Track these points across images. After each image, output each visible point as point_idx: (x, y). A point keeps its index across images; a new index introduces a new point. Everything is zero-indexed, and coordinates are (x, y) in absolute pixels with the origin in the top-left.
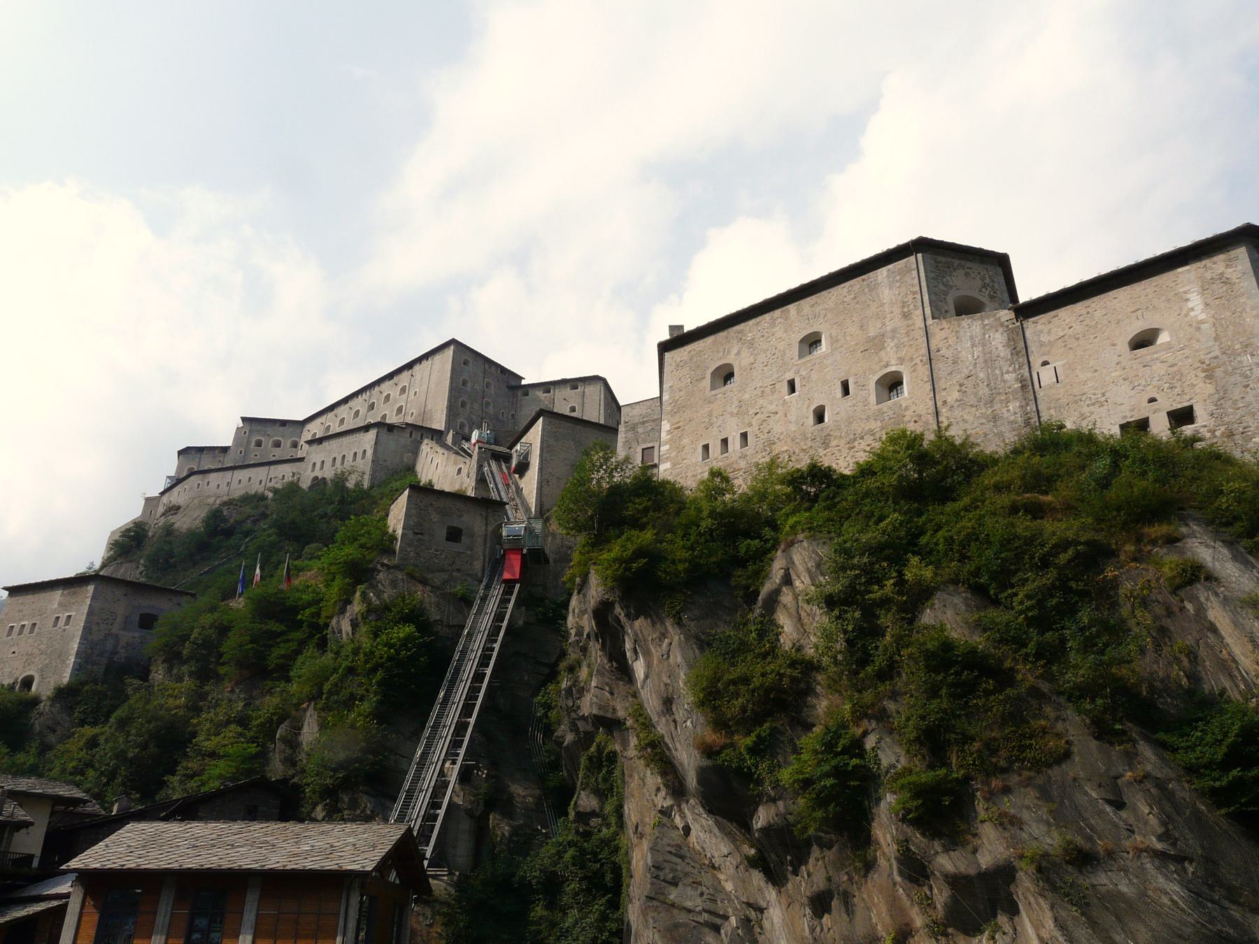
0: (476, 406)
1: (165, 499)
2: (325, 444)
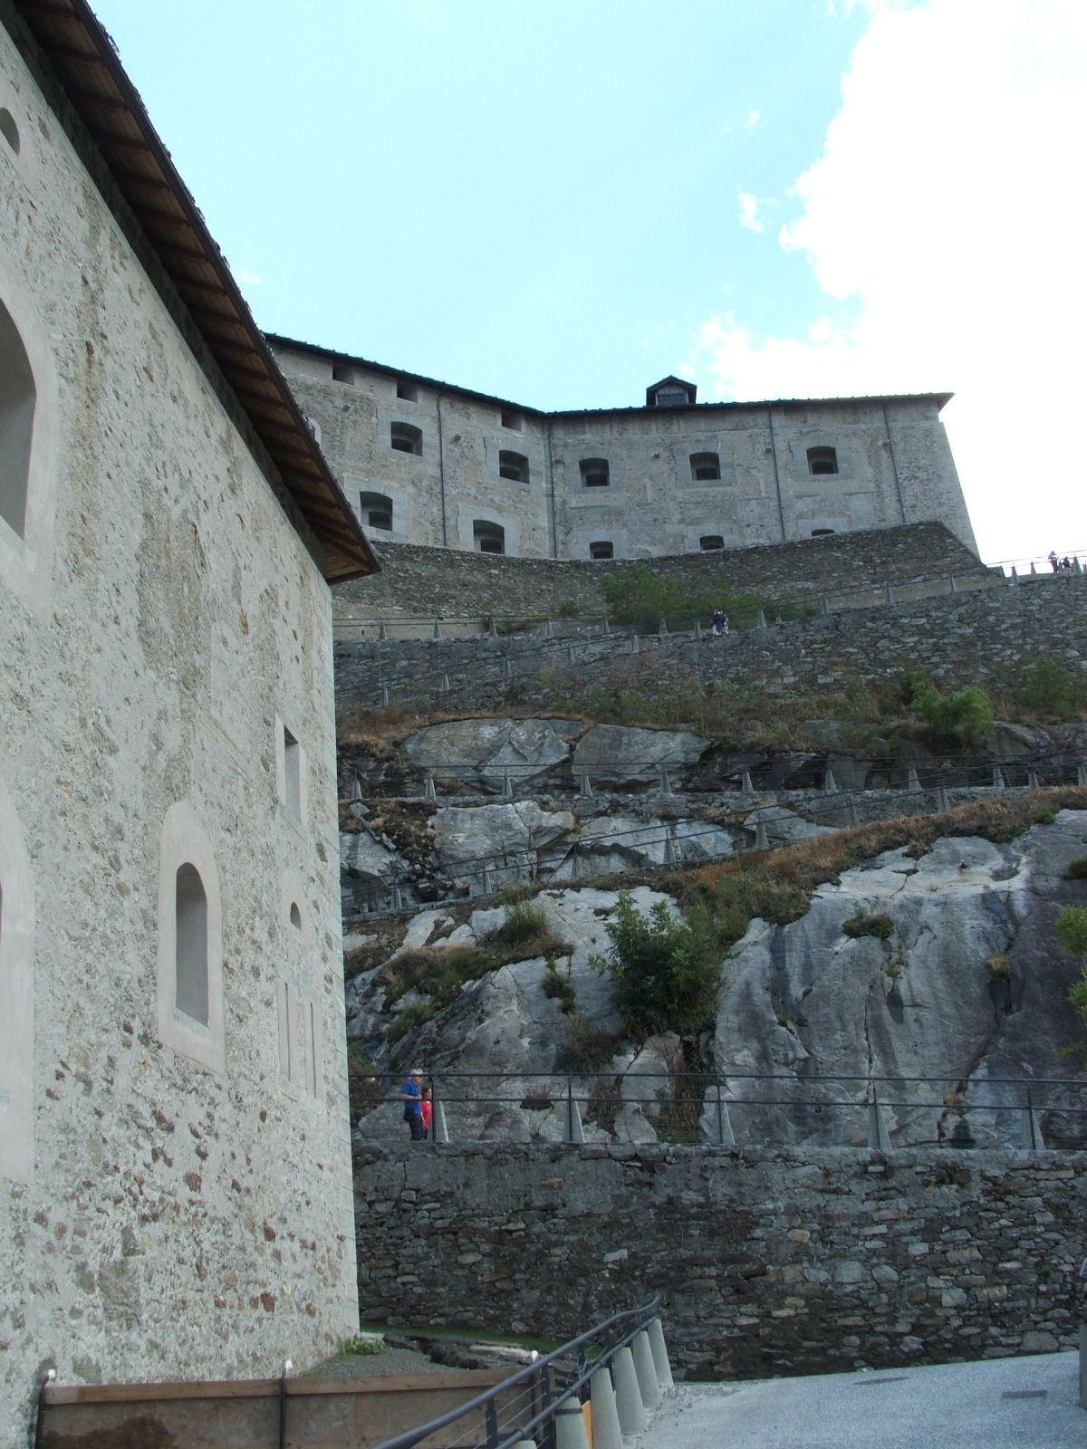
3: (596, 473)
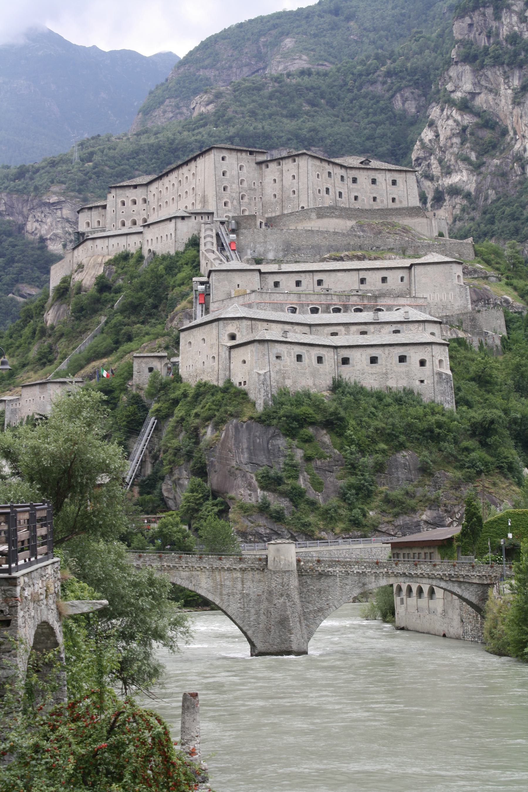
0: (234, 186)
1: (76, 252)
2: (151, 227)
3: (355, 180)
